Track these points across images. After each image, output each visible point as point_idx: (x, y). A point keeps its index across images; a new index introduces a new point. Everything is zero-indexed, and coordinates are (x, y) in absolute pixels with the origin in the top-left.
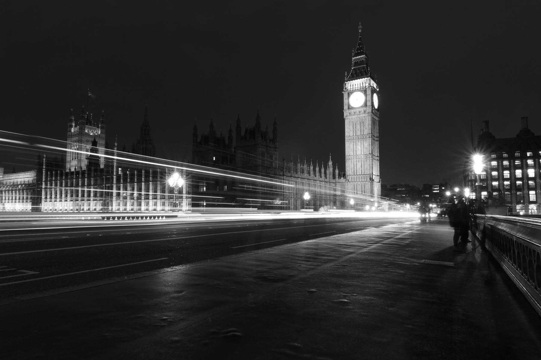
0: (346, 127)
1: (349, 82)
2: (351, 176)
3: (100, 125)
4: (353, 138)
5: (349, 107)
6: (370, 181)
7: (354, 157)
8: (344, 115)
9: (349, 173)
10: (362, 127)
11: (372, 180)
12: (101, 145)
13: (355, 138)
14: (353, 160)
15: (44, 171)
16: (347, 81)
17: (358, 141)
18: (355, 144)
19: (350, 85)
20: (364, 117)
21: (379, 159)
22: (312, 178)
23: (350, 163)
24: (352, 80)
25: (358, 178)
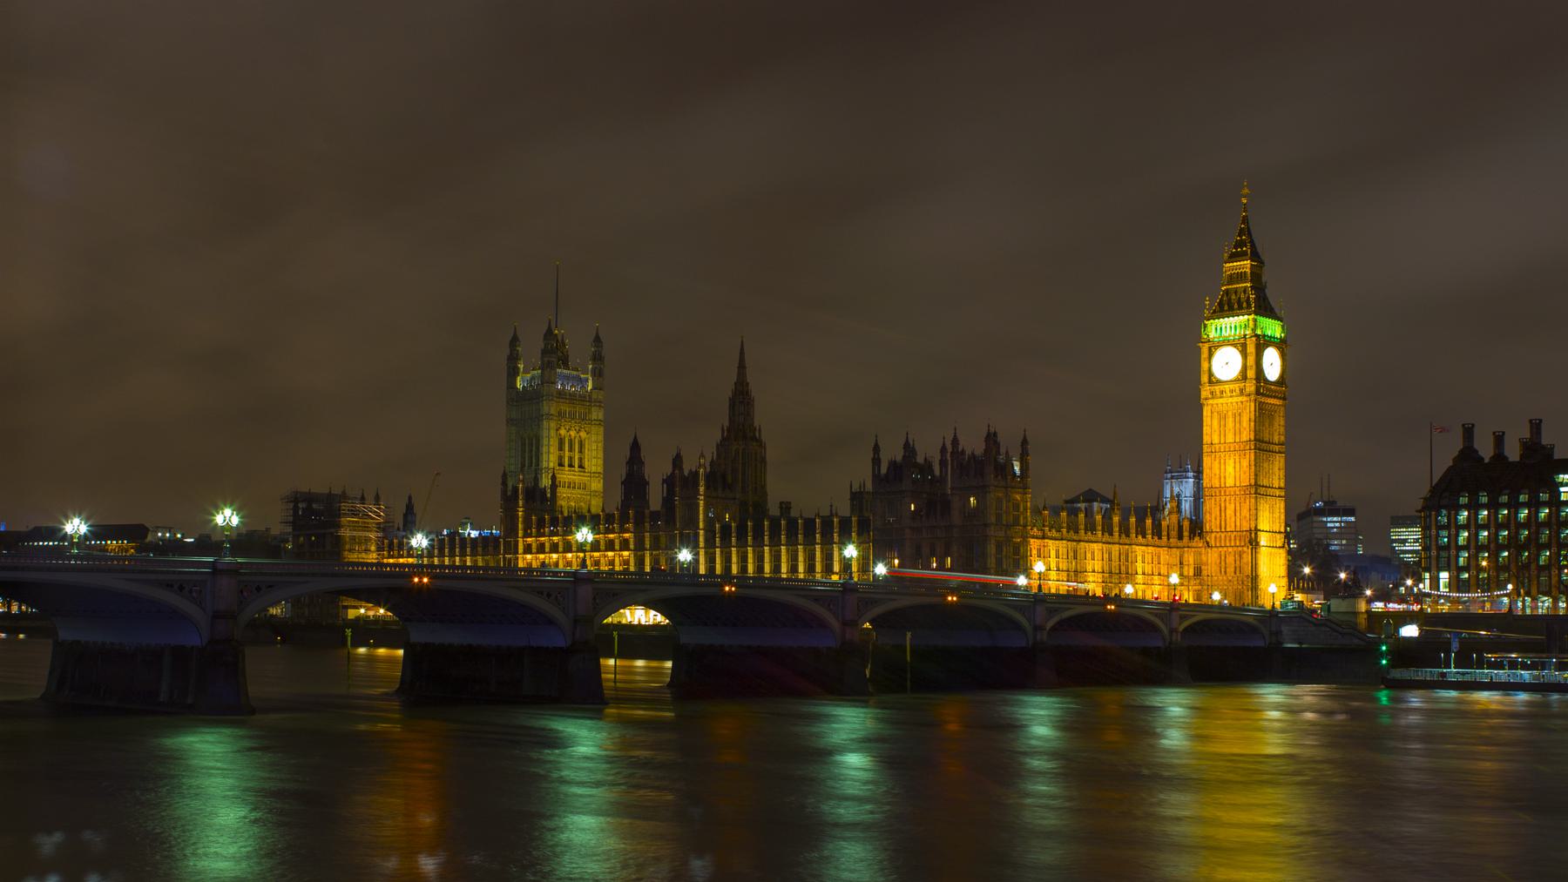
0: (1205, 424)
1: (1212, 321)
2: (1213, 535)
3: (591, 366)
4: (1220, 448)
5: (1212, 380)
6: (1250, 547)
7: (1220, 492)
8: (1202, 397)
9: (1210, 527)
10: (1237, 425)
11: (1254, 543)
12: (593, 422)
13: (1222, 447)
14: (1218, 498)
15: (520, 513)
16: (1209, 320)
17: (1230, 456)
18: (1222, 461)
19: (1216, 329)
20: (1242, 402)
21: (1283, 494)
22: (1117, 540)
23: (1213, 505)
24: (1219, 319)
25: (1228, 539)
